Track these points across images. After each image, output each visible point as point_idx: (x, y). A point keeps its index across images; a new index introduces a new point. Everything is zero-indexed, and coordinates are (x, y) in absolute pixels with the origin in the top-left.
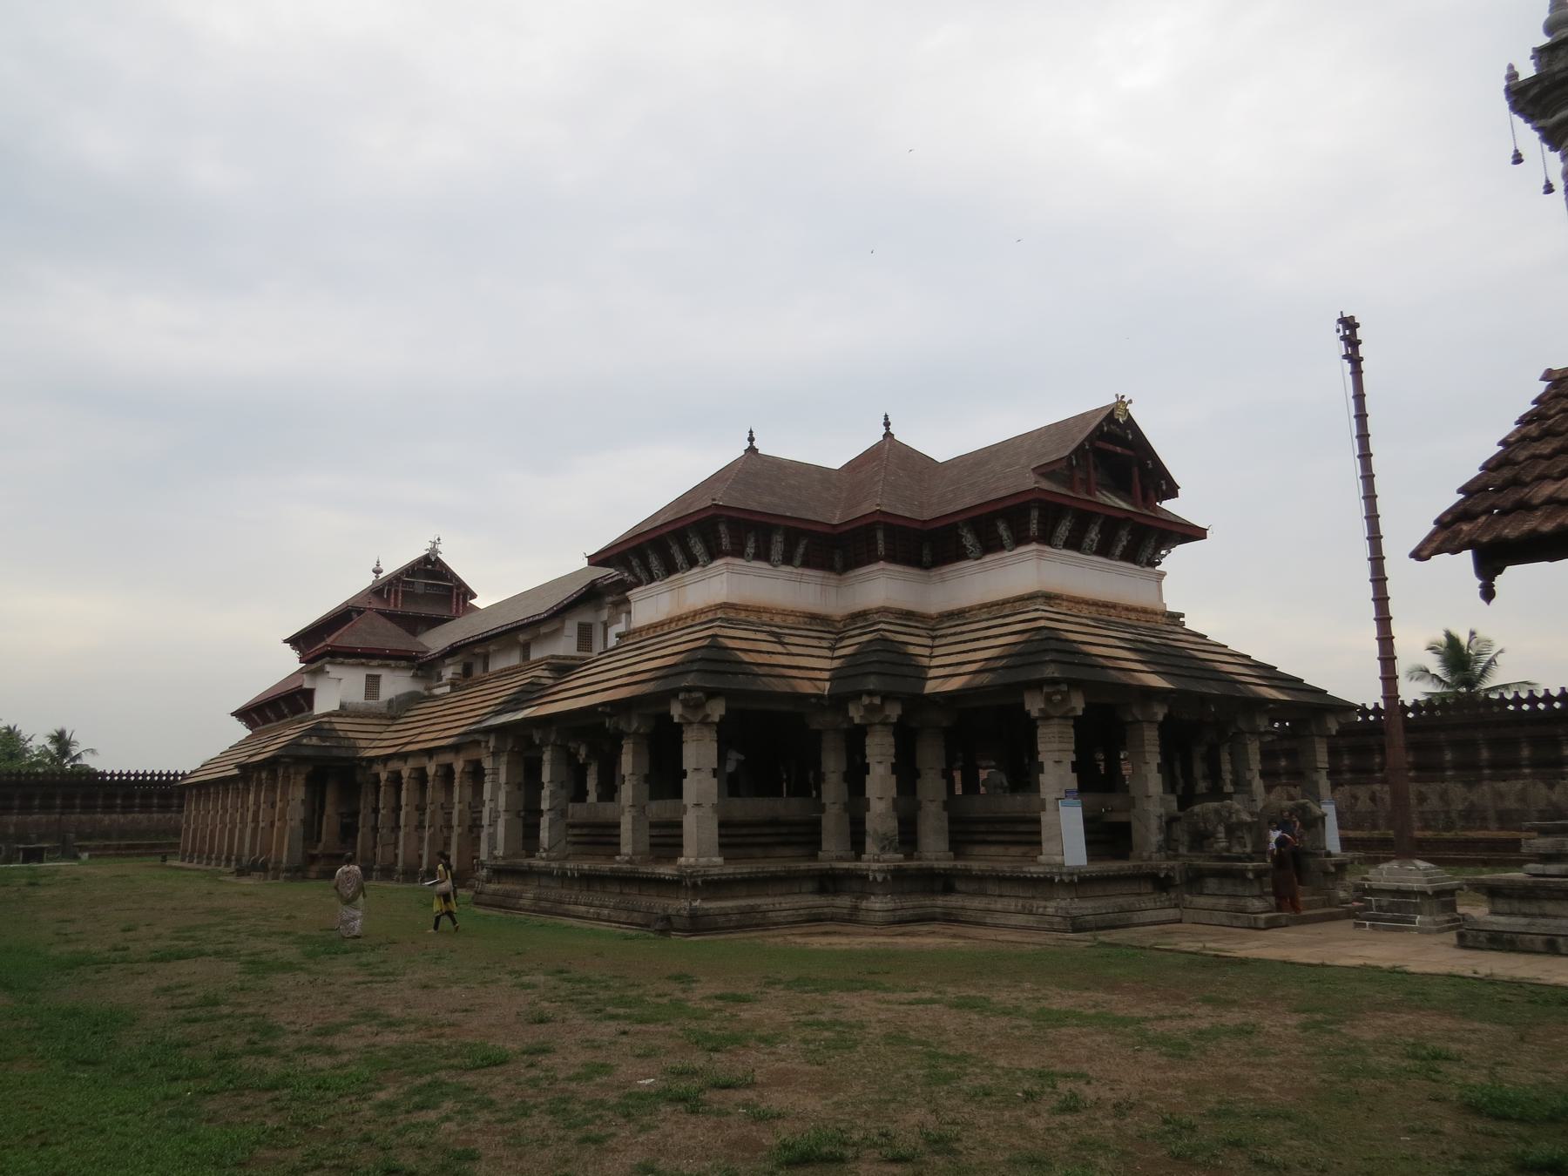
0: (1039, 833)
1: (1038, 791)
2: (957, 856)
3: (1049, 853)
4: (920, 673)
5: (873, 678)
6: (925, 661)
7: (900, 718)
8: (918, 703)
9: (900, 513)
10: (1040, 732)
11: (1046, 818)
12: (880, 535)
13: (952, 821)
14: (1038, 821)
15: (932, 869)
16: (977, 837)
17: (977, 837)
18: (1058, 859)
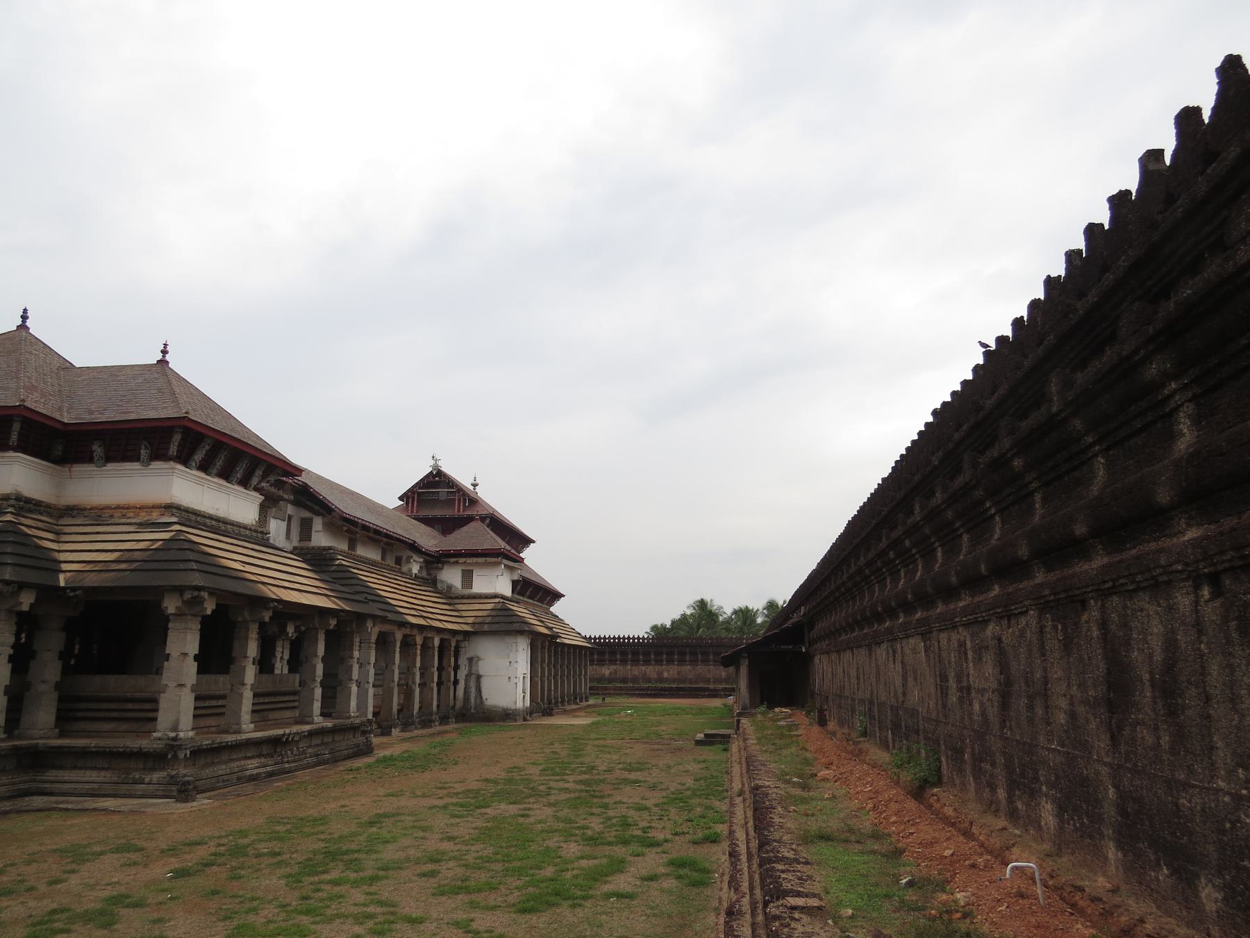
0: (156, 710)
1: (159, 672)
2: (62, 735)
3: (162, 729)
4: (53, 567)
5: (9, 569)
6: (56, 555)
7: (32, 605)
8: (49, 593)
9: (44, 411)
10: (170, 625)
11: (164, 702)
12: (16, 426)
13: (61, 700)
14: (155, 701)
15: (36, 746)
16: (80, 714)
17: (80, 714)
18: (173, 735)
